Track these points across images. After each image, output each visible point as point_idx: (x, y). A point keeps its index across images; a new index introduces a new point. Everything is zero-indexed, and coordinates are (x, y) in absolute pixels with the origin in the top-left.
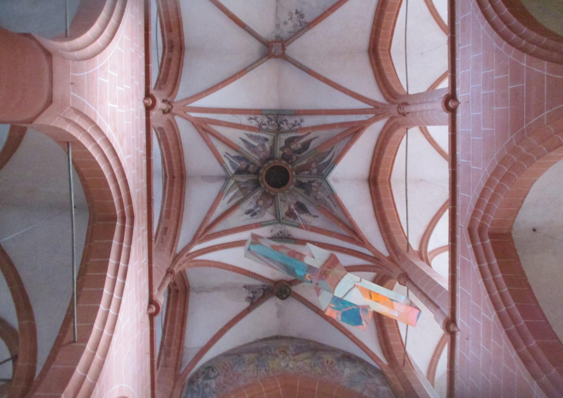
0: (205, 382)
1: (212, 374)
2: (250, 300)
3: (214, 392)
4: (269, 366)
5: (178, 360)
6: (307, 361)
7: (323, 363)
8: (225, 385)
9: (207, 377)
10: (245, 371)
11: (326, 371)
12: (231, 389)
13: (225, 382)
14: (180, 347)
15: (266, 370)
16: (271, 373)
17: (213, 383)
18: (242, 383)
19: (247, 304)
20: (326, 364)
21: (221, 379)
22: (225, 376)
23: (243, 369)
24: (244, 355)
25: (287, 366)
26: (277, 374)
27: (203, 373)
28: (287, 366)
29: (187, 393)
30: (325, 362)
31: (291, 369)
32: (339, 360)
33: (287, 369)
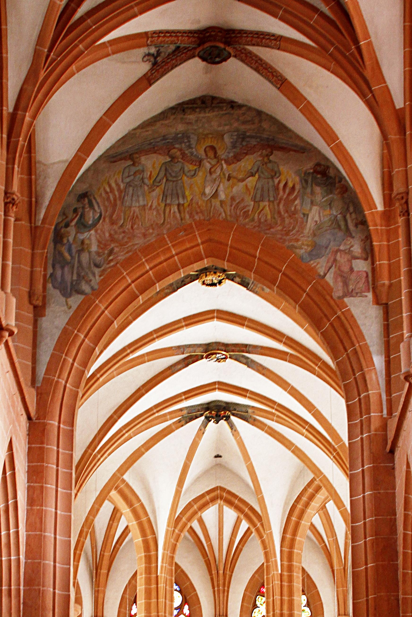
0: (81, 237)
1: (90, 217)
2: (152, 59)
3: (97, 266)
4: (184, 197)
5: (30, 197)
6: (251, 181)
7: (277, 188)
8: (113, 245)
9: (83, 226)
10: (144, 206)
11: (279, 212)
12: (121, 257)
13: (112, 239)
14: (30, 167)
15: (179, 205)
16: (187, 217)
17: (91, 237)
18: (139, 242)
19: (144, 68)
20: (281, 193)
21: (105, 226)
22: (113, 223)
23: (141, 203)
24: (143, 159)
25: (216, 195)
26: (197, 217)
27: (75, 211)
28: (216, 195)
29: (54, 267)
30: (281, 185)
31: (222, 202)
32: (306, 181)
33: (216, 203)
